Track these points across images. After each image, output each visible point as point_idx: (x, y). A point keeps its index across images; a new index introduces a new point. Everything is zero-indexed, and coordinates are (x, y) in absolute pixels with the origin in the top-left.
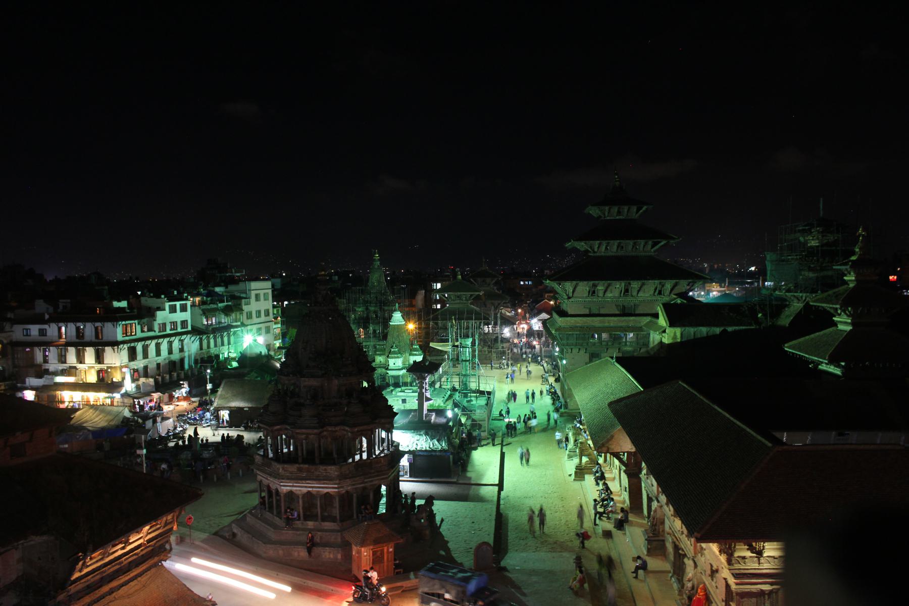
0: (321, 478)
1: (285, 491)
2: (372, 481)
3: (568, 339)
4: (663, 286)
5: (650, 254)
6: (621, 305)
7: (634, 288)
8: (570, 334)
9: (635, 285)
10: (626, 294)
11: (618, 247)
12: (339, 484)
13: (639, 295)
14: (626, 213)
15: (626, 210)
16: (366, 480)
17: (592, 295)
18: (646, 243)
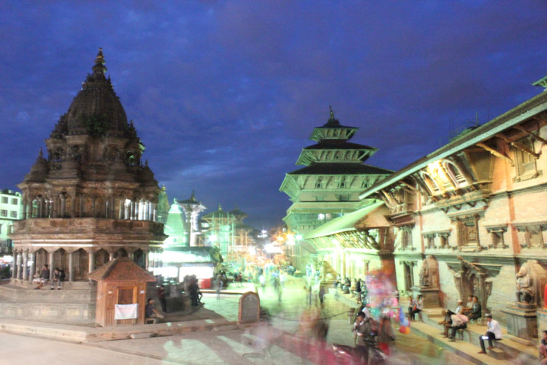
0: (74, 232)
1: (35, 248)
2: (130, 243)
3: (301, 218)
4: (368, 181)
5: (356, 162)
6: (339, 194)
7: (348, 182)
8: (302, 214)
9: (349, 178)
10: (342, 187)
11: (335, 156)
12: (93, 238)
13: (351, 188)
14: (339, 135)
15: (339, 132)
16: (124, 241)
17: (317, 187)
18: (355, 153)
